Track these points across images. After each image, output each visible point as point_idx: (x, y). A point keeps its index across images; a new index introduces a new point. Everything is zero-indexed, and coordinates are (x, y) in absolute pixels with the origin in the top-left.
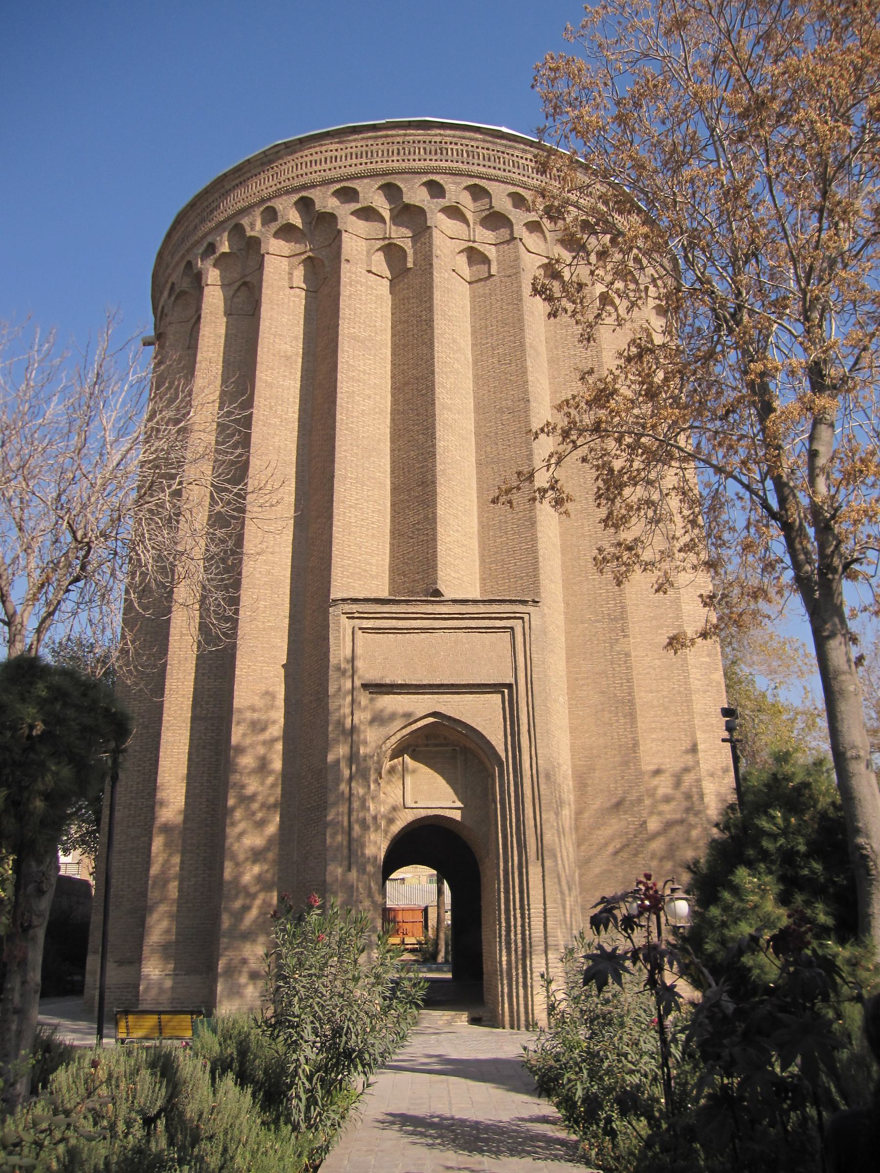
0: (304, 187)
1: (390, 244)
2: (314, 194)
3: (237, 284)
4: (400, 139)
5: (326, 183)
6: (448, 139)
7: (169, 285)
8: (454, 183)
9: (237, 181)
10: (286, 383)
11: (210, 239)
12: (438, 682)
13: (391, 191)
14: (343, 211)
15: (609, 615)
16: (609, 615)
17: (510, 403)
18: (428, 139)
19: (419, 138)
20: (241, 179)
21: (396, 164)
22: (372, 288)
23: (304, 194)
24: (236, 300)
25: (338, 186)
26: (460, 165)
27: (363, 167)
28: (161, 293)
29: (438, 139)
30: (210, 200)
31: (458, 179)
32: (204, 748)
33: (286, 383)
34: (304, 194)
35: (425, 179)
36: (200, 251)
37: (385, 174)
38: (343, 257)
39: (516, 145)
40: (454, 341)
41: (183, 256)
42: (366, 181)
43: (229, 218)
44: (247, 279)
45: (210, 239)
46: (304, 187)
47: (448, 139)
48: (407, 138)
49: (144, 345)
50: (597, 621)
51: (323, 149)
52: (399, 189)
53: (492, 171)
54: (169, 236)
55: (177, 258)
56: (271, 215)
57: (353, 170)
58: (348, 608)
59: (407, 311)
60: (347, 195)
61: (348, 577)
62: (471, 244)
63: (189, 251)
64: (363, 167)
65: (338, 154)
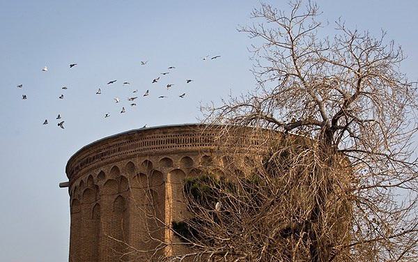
2: (153, 160)
5: (158, 154)
13: (187, 160)
21: (190, 148)
28: (75, 180)
30: (102, 147)
36: (98, 173)
37: (185, 152)
38: (166, 197)
41: (88, 171)
43: (111, 162)
49: (61, 187)
51: (156, 135)
54: (79, 153)
56: (132, 166)
60: (168, 161)
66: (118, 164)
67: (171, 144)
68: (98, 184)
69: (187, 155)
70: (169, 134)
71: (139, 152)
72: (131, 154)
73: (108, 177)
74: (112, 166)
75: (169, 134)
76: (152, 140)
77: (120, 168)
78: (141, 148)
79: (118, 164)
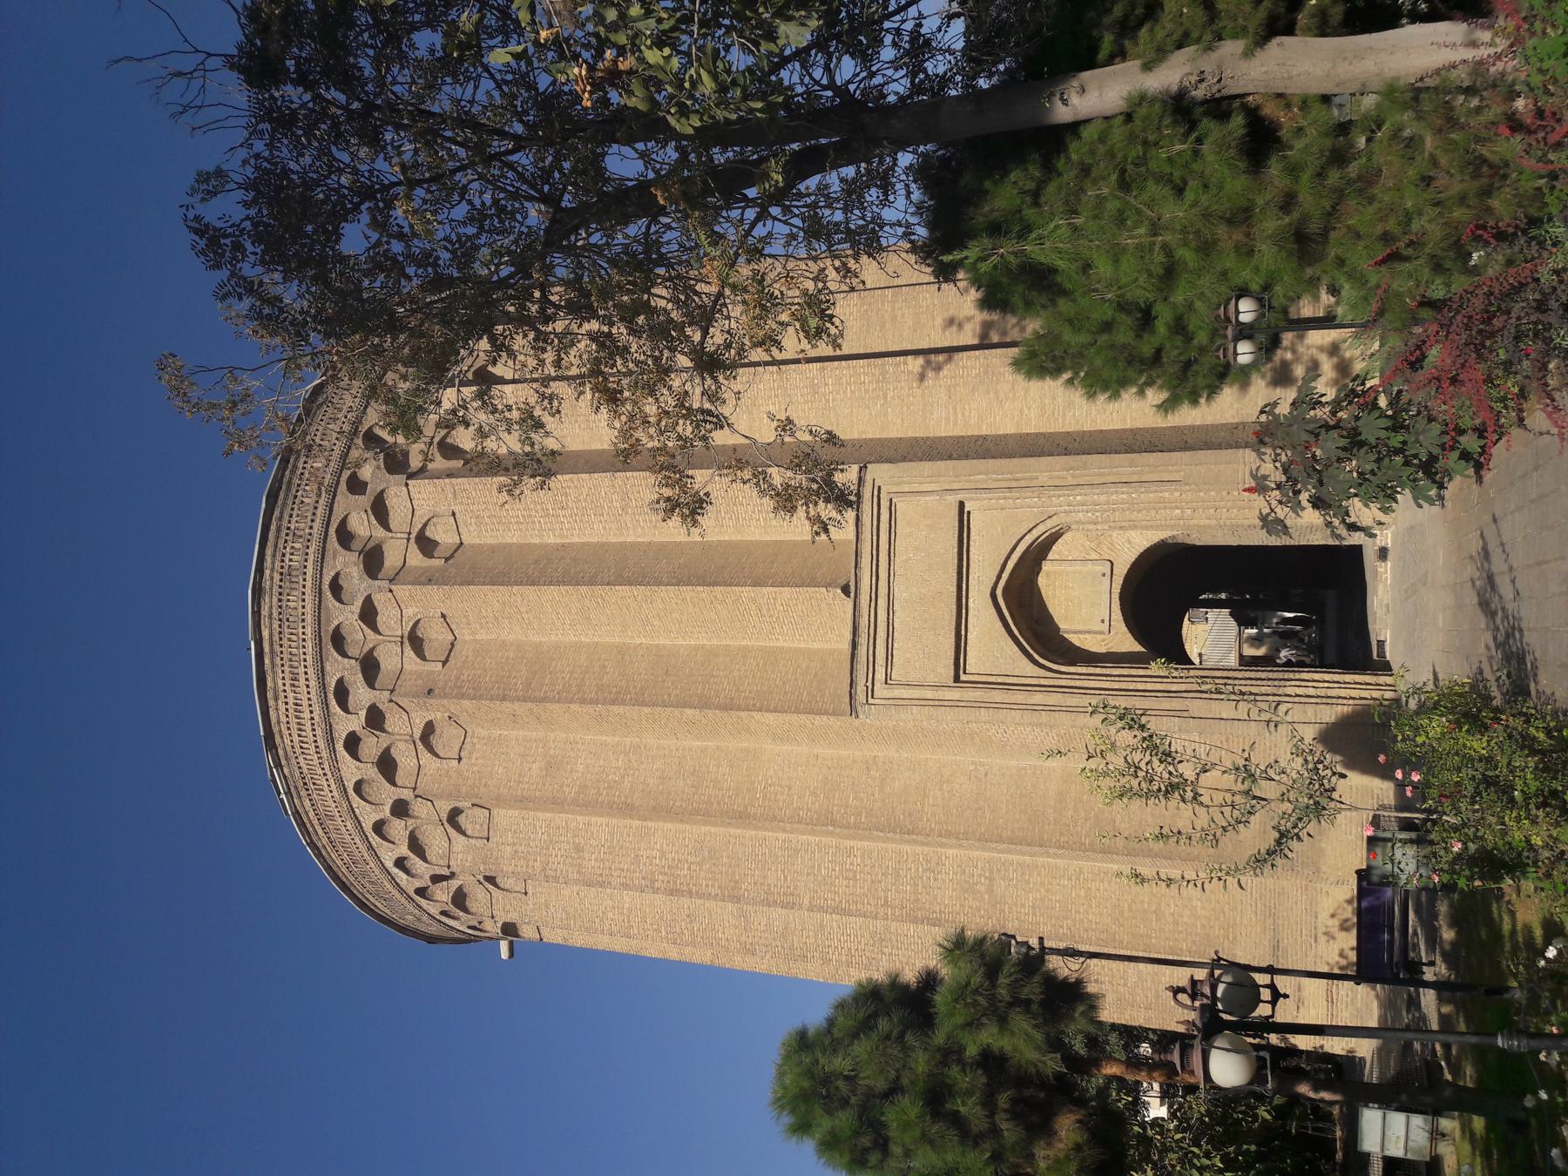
0: (331, 741)
1: (410, 639)
3: (450, 830)
4: (276, 624)
6: (278, 564)
7: (443, 919)
8: (334, 557)
9: (320, 832)
10: (581, 768)
11: (389, 864)
12: (954, 589)
14: (361, 696)
15: (878, 382)
16: (878, 382)
17: (615, 497)
18: (275, 588)
19: (275, 600)
20: (316, 822)
21: (309, 630)
22: (465, 661)
23: (340, 746)
24: (469, 832)
25: (333, 702)
26: (311, 551)
27: (310, 671)
29: (277, 577)
31: (329, 554)
32: (1028, 882)
33: (581, 768)
34: (340, 746)
35: (328, 594)
39: (285, 480)
40: (537, 562)
42: (328, 667)
44: (444, 817)
45: (389, 864)
46: (331, 741)
47: (278, 564)
48: (275, 615)
50: (885, 398)
51: (284, 719)
52: (338, 627)
53: (319, 512)
55: (410, 907)
57: (313, 683)
58: (861, 697)
59: (496, 619)
61: (823, 695)
62: (412, 541)
63: (402, 891)
64: (310, 671)
65: (291, 701)
66: (368, 826)
67: (302, 682)
68: (427, 877)
69: (327, 639)
70: (280, 682)
71: (326, 766)
72: (333, 787)
73: (404, 850)
74: (375, 840)
75: (280, 682)
76: (295, 733)
77: (376, 817)
78: (316, 762)
79: (368, 826)
